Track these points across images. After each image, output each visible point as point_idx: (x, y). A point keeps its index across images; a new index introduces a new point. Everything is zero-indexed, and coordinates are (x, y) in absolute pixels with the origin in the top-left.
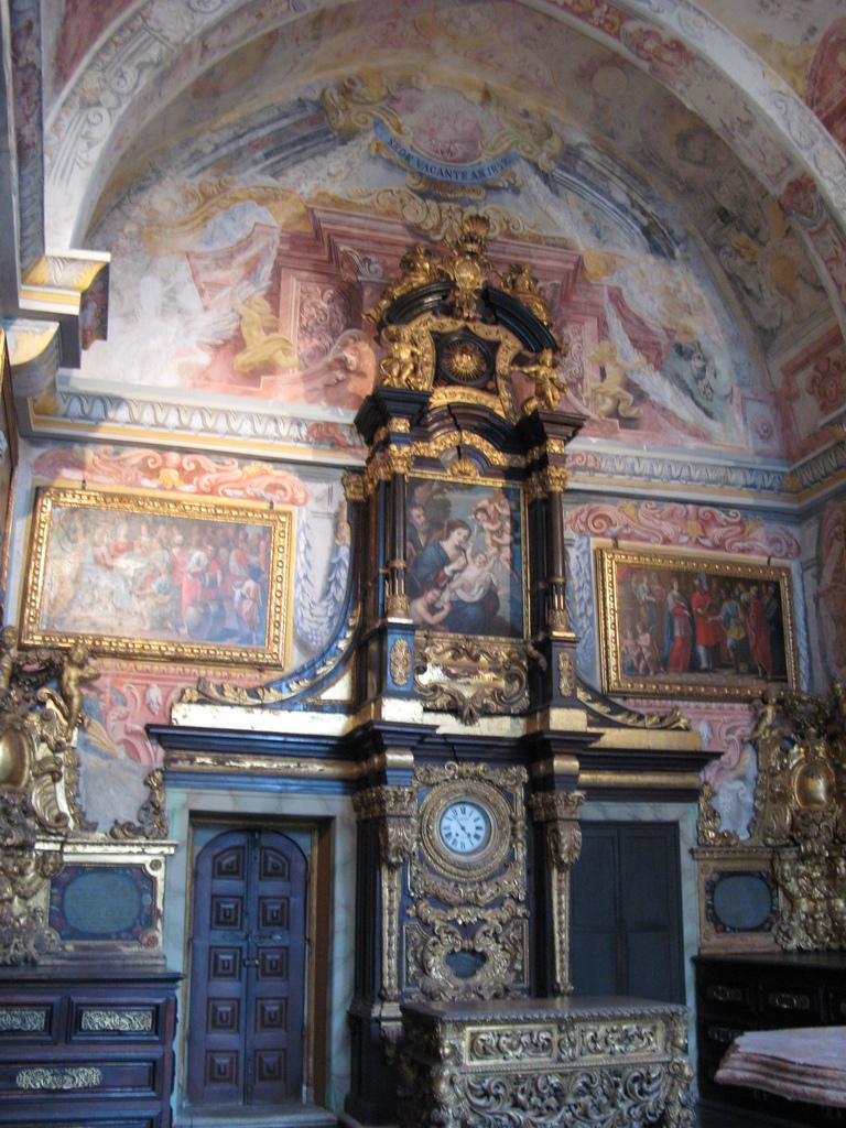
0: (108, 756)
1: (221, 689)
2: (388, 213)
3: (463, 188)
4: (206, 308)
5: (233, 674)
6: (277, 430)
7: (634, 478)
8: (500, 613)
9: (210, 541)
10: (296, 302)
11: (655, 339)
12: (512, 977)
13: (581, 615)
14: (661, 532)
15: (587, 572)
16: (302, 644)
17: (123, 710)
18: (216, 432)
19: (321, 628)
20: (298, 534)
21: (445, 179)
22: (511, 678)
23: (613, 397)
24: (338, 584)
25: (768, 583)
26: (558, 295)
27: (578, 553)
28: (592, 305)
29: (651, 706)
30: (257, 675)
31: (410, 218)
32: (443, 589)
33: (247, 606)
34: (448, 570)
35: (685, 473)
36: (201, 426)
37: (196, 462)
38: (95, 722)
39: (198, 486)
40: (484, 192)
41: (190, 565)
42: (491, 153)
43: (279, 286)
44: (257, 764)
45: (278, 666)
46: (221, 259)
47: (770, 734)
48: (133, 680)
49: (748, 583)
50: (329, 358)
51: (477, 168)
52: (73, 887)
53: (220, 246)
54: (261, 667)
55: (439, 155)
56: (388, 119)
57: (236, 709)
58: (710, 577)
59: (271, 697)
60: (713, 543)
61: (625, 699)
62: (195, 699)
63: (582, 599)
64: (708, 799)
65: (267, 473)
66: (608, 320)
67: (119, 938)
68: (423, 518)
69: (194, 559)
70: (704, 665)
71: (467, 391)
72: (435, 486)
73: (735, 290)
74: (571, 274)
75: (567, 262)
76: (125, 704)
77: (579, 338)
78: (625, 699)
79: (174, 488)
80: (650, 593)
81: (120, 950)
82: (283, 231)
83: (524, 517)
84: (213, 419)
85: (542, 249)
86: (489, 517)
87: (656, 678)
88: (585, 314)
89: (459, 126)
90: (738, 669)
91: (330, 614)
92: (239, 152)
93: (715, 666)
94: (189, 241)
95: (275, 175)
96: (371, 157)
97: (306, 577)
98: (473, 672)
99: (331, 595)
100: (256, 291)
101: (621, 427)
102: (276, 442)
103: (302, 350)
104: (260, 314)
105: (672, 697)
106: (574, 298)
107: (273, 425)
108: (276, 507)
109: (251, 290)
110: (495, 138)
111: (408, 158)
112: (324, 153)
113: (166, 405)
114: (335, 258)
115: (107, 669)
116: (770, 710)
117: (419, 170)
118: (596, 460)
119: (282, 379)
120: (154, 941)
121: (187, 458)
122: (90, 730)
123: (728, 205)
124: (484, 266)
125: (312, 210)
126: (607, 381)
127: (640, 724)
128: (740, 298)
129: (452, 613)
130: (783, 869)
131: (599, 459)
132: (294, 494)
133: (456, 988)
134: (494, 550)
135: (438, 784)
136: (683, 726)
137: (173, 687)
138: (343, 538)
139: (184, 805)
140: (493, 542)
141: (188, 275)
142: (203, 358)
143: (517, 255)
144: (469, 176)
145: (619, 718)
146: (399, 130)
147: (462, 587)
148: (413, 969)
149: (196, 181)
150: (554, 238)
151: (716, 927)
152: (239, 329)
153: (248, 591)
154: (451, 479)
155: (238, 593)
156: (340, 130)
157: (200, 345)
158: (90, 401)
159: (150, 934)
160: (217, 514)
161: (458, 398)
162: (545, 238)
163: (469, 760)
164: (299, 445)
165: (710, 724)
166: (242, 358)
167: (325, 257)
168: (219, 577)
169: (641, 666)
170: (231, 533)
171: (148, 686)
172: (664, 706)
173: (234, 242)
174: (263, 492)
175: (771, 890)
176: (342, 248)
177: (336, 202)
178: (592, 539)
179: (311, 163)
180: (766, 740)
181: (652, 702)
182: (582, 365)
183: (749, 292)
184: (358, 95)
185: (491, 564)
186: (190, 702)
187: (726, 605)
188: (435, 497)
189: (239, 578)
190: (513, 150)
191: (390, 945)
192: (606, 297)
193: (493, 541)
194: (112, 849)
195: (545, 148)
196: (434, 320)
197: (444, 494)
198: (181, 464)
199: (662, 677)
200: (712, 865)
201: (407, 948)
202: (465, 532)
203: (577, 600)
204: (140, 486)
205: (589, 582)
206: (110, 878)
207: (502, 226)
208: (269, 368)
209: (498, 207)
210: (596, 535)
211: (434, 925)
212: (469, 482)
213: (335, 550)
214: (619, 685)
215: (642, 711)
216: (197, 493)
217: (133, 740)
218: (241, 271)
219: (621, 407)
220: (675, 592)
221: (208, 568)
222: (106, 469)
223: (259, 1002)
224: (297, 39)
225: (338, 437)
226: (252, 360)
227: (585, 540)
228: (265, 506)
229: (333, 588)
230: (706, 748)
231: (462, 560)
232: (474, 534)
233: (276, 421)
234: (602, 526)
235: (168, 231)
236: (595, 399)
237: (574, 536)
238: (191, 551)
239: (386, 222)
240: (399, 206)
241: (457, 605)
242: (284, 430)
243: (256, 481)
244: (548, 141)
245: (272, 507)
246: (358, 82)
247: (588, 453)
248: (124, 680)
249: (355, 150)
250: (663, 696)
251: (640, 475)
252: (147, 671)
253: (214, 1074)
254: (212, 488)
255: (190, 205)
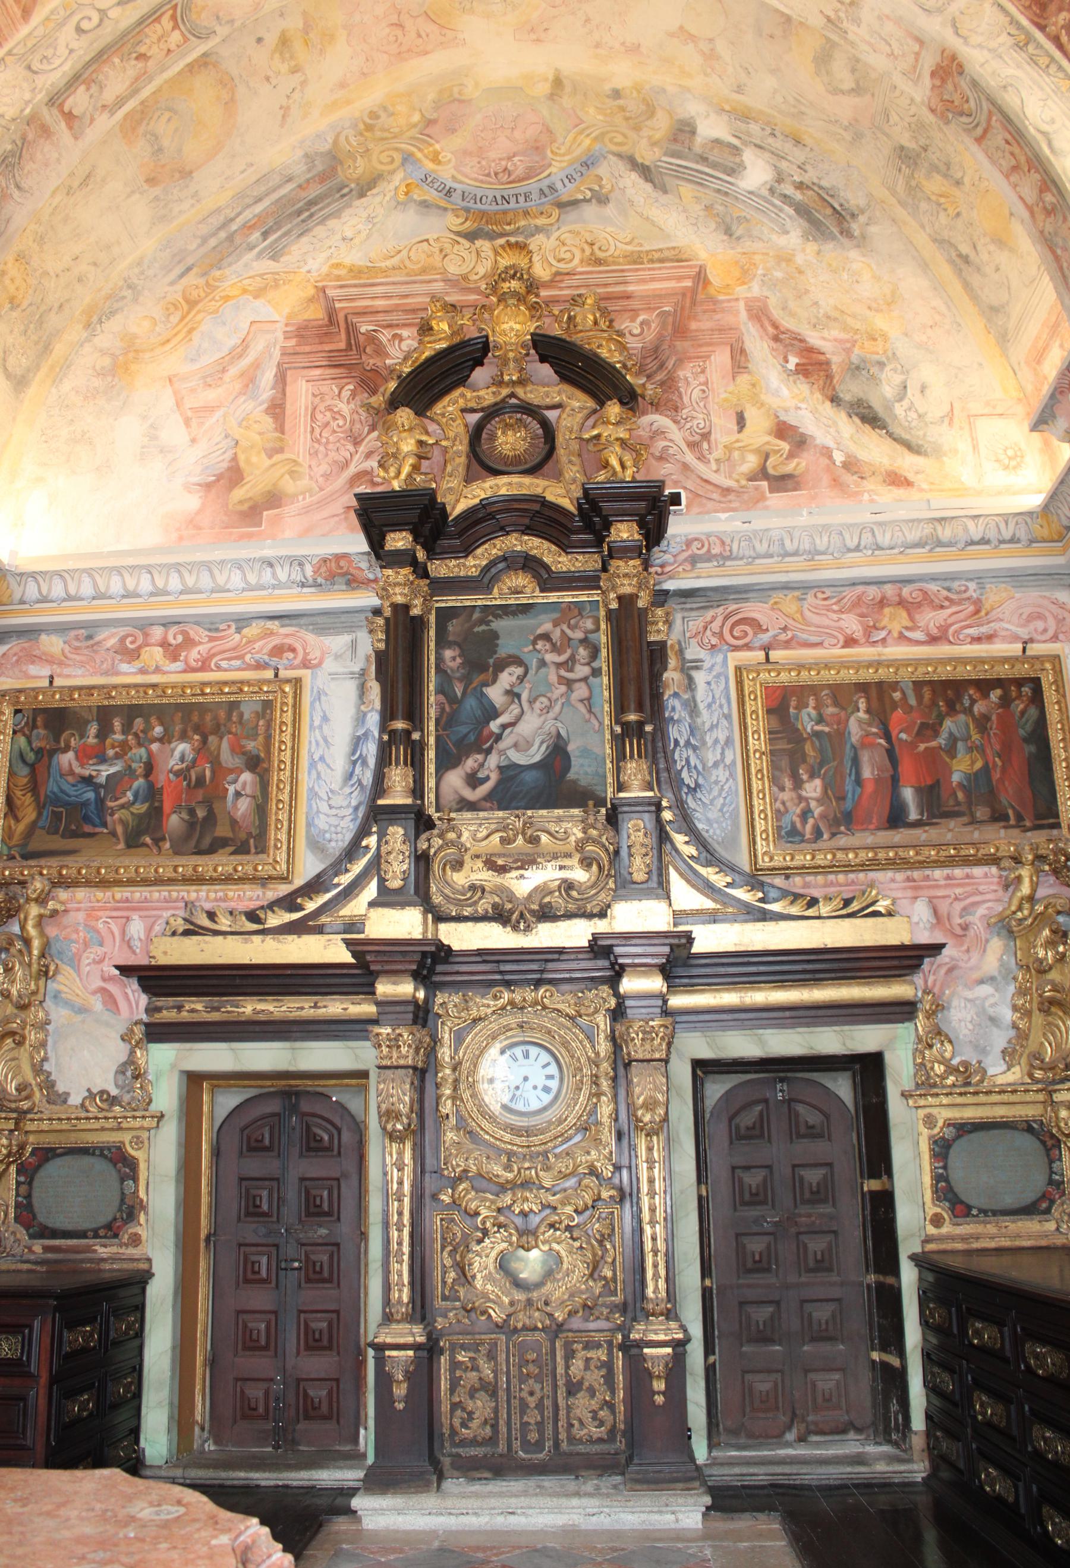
0: (82, 1010)
1: (212, 916)
2: (424, 271)
3: (526, 213)
4: (193, 441)
5: (231, 894)
6: (274, 574)
7: (787, 559)
8: (571, 775)
9: (197, 729)
10: (306, 409)
11: (822, 357)
12: (597, 1288)
13: (716, 765)
14: (841, 629)
15: (724, 701)
16: (316, 846)
17: (100, 951)
18: (200, 592)
19: (343, 824)
20: (312, 703)
21: (500, 207)
22: (586, 862)
23: (757, 451)
24: (365, 763)
25: (1019, 682)
26: (670, 328)
27: (709, 678)
28: (721, 330)
29: (832, 884)
30: (259, 892)
31: (454, 269)
32: (488, 752)
33: (244, 806)
34: (494, 726)
35: (867, 539)
36: (180, 587)
37: (185, 633)
38: (66, 970)
39: (186, 663)
40: (556, 212)
41: (172, 763)
42: (567, 158)
43: (284, 394)
44: (260, 1006)
45: (285, 879)
46: (210, 375)
47: (1032, 909)
48: (108, 913)
49: (984, 686)
50: (352, 470)
51: (546, 182)
52: (42, 1173)
53: (207, 359)
54: (265, 881)
55: (493, 180)
56: (420, 150)
57: (230, 937)
58: (918, 685)
59: (274, 920)
60: (928, 634)
61: (787, 877)
62: (181, 930)
63: (716, 741)
64: (930, 1015)
65: (272, 634)
66: (749, 345)
67: (96, 1236)
68: (459, 660)
69: (177, 754)
70: (913, 815)
71: (515, 479)
72: (476, 615)
73: (951, 262)
74: (689, 295)
75: (680, 279)
76: (101, 945)
77: (702, 379)
78: (787, 877)
79: (158, 670)
80: (820, 720)
81: (95, 1251)
82: (287, 325)
83: (603, 638)
84: (194, 578)
85: (643, 269)
86: (554, 645)
87: (834, 843)
88: (710, 344)
89: (517, 134)
90: (972, 815)
91: (354, 803)
92: (230, 238)
93: (932, 815)
94: (173, 362)
95: (274, 258)
96: (398, 203)
97: (322, 758)
98: (527, 862)
99: (355, 779)
100: (254, 408)
101: (771, 492)
102: (276, 592)
103: (315, 469)
104: (260, 434)
105: (863, 867)
106: (693, 325)
107: (269, 570)
108: (283, 674)
109: (250, 405)
110: (570, 137)
111: (449, 193)
112: (336, 214)
113: (134, 567)
114: (356, 343)
115: (80, 902)
116: (1025, 872)
117: (465, 204)
118: (723, 543)
119: (290, 510)
120: (136, 1240)
121: (174, 629)
122: (59, 978)
123: (906, 141)
124: (534, 307)
125: (323, 290)
126: (746, 430)
127: (810, 912)
128: (959, 272)
129: (499, 783)
130: (1057, 1117)
131: (728, 541)
132: (306, 654)
133: (512, 1304)
134: (563, 689)
135: (480, 1019)
136: (883, 911)
137: (160, 917)
138: (372, 702)
139: (173, 1066)
140: (562, 680)
141: (171, 402)
142: (193, 502)
143: (606, 285)
144: (535, 196)
145: (776, 907)
146: (435, 159)
147: (515, 745)
148: (453, 1275)
149: (179, 287)
150: (661, 250)
151: (952, 1209)
152: (235, 458)
153: (244, 784)
154: (498, 602)
155: (231, 789)
156: (357, 181)
157: (188, 488)
158: (76, 576)
159: (130, 1231)
160: (203, 694)
161: (503, 491)
162: (647, 252)
163: (528, 982)
164: (305, 590)
165: (931, 900)
166: (239, 493)
167: (342, 345)
168: (208, 773)
169: (809, 827)
170: (222, 714)
171: (128, 918)
172: (853, 883)
173: (225, 351)
174: (266, 657)
175: (1048, 1150)
176: (363, 330)
177: (356, 271)
178: (729, 654)
179: (320, 231)
180: (1025, 919)
181: (831, 877)
182: (708, 414)
183: (966, 259)
184: (383, 130)
185: (557, 708)
186: (174, 934)
187: (948, 724)
188: (476, 630)
189: (231, 771)
190: (597, 146)
191: (400, 1244)
192: (743, 315)
193: (560, 677)
194: (83, 1125)
195: (645, 132)
196: (469, 395)
197: (488, 623)
198: (165, 638)
199: (843, 841)
200: (943, 1115)
201: (443, 1248)
202: (519, 671)
203: (709, 740)
204: (118, 673)
205: (728, 717)
206: (87, 1160)
207: (583, 251)
208: (273, 499)
209: (576, 227)
210: (736, 648)
211: (477, 1214)
212: (525, 602)
213: (360, 718)
214: (771, 859)
215: (816, 893)
216: (185, 671)
217: (110, 987)
218: (238, 386)
219: (770, 463)
220: (861, 714)
221: (194, 761)
222: (78, 658)
223: (302, 1316)
224: (268, 79)
225: (352, 571)
226: (250, 495)
227: (719, 658)
228: (269, 674)
229: (358, 769)
230: (924, 937)
231: (515, 709)
232: (532, 672)
233: (271, 565)
234: (746, 634)
235: (147, 355)
236: (729, 459)
237: (702, 654)
238: (173, 745)
239: (422, 282)
240: (438, 257)
241: (509, 772)
242: (282, 575)
243: (257, 646)
244: (648, 123)
245: (276, 675)
246: (383, 115)
247: (708, 535)
248: (100, 913)
249: (378, 199)
250: (848, 868)
251: (796, 554)
252: (127, 900)
253: (247, 1411)
254: (204, 663)
255: (172, 318)
